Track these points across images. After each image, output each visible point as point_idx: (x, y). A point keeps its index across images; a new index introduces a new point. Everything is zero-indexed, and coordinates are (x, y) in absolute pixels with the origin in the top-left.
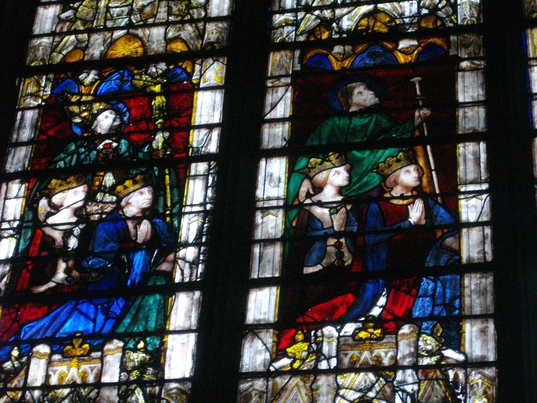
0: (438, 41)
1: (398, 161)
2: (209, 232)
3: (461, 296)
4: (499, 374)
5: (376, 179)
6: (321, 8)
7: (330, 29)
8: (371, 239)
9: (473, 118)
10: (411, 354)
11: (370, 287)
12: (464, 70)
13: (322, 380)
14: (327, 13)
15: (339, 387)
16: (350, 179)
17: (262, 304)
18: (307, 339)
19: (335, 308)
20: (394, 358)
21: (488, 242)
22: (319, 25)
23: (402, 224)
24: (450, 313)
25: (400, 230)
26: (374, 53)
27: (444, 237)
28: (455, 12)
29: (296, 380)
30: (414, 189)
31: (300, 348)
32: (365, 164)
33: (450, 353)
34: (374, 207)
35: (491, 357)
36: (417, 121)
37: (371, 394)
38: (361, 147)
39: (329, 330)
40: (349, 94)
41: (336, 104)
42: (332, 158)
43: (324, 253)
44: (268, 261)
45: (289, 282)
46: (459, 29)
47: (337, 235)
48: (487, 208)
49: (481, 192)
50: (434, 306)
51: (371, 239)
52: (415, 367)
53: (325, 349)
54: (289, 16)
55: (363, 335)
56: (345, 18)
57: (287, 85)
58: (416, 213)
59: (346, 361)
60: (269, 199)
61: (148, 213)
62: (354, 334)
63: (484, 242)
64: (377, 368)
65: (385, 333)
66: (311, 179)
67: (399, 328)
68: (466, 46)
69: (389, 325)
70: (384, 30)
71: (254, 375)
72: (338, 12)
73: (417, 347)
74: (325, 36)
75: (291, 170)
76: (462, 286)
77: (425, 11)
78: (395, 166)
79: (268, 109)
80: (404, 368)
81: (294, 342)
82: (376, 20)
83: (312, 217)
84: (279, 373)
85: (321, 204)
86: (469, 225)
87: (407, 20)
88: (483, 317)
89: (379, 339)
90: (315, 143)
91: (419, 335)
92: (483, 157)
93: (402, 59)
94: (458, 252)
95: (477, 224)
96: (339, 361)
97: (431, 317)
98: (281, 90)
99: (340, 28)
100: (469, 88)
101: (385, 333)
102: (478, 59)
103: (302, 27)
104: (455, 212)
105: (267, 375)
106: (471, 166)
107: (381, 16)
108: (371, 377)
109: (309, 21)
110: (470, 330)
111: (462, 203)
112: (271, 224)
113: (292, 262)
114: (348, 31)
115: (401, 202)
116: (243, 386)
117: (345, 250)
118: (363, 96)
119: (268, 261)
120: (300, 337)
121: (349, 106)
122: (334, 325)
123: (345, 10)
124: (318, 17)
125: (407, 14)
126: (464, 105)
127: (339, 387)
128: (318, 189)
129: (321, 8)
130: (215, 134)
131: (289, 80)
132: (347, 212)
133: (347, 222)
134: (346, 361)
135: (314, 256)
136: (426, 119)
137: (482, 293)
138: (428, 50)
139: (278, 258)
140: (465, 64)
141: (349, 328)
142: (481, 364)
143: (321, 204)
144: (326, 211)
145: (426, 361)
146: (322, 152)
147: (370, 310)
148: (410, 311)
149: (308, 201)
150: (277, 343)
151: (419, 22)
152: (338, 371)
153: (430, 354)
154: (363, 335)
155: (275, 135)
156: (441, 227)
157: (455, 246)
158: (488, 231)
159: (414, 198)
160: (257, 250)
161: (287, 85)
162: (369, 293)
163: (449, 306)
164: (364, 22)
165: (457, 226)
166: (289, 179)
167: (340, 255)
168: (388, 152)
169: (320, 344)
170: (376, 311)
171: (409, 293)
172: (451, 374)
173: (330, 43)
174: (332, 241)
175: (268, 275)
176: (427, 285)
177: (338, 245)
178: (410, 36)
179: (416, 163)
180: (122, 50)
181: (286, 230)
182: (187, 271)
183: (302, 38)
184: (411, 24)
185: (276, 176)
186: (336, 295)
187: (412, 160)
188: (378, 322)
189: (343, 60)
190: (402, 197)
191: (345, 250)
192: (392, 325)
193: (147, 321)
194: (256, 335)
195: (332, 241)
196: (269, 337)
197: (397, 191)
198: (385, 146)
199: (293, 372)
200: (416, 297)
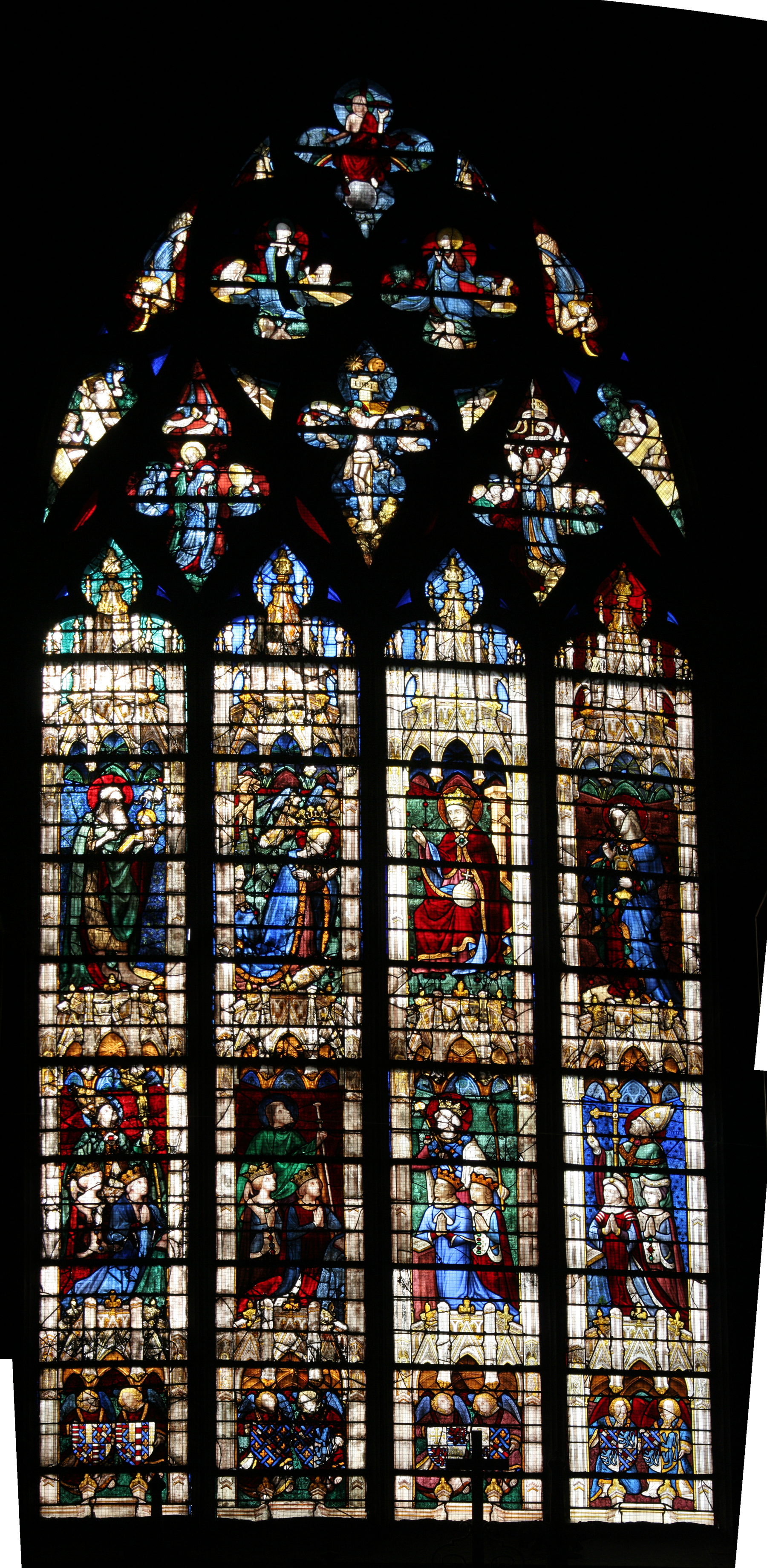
0: (332, 1072)
1: (307, 1174)
2: (189, 1219)
3: (345, 1284)
4: (367, 1341)
5: (293, 1187)
6: (251, 1026)
7: (257, 1048)
8: (291, 1235)
9: (354, 1145)
10: (316, 1323)
11: (291, 1271)
12: (348, 1100)
13: (265, 1336)
14: (254, 1032)
15: (275, 1342)
16: (276, 1185)
17: (226, 1279)
18: (254, 1307)
19: (271, 1286)
20: (306, 1324)
21: (361, 1245)
22: (249, 1043)
23: (308, 1226)
24: (338, 1295)
25: (309, 1230)
26: (289, 1076)
27: (335, 1239)
28: (343, 1045)
29: (249, 1335)
30: (316, 1198)
31: (250, 1313)
32: (286, 1174)
33: (338, 1323)
34: (292, 1210)
35: (362, 1330)
36: (318, 1142)
37: (294, 1348)
38: (283, 1160)
39: (268, 1301)
40: (273, 1112)
41: (264, 1119)
42: (264, 1166)
43: (262, 1244)
44: (227, 1247)
45: (241, 1263)
46: (347, 1063)
47: (269, 1230)
48: (361, 1219)
49: (358, 1206)
50: (330, 1289)
51: (291, 1235)
52: (319, 1332)
53: (266, 1315)
54: (227, 1030)
55: (288, 1306)
56: (267, 1038)
57: (230, 1097)
58: (318, 1218)
59: (279, 1323)
60: (225, 1196)
61: (147, 1199)
62: (283, 1305)
63: (359, 1245)
64: (297, 1331)
65: (301, 1306)
66: (251, 1182)
67: (309, 1304)
68: (350, 1079)
69: (303, 1301)
70: (295, 1055)
71: (224, 1330)
72: (264, 1031)
73: (319, 1318)
74: (254, 1055)
75: (238, 1174)
76: (346, 1277)
77: (322, 1040)
78: (305, 1178)
79: (219, 1118)
80: (312, 1332)
81: (247, 1308)
82: (289, 1044)
83: (253, 1214)
84: (239, 1329)
85: (259, 1205)
86: (351, 1231)
87: (310, 1047)
88: (358, 1301)
89: (297, 1310)
90: (253, 1152)
91: (321, 1309)
92: (360, 1177)
93: (307, 1084)
94: (344, 1251)
95: (355, 1231)
96: (275, 1324)
97: (328, 1298)
98: (226, 1101)
99: (264, 1047)
100: (352, 1118)
101: (301, 1306)
102: (358, 1092)
103: (237, 1044)
104: (342, 1221)
105: (233, 1330)
106: (352, 1184)
107: (292, 1040)
108: (293, 1336)
109: (242, 1038)
110: (350, 1308)
111: (346, 1212)
112: (227, 1217)
113: (242, 1248)
114: (270, 1052)
115: (308, 1208)
116: (219, 1337)
117: (275, 1242)
118: (283, 1115)
119: (227, 1247)
120: (251, 1305)
121: (273, 1123)
122: (270, 1298)
123: (267, 1030)
124: (248, 1035)
125: (310, 1042)
126: (349, 1132)
127: (275, 1342)
128: (256, 1191)
129: (251, 1026)
130: (185, 1134)
131: (230, 1093)
132: (275, 1212)
133: (276, 1221)
134: (279, 1323)
135: (256, 1245)
136: (324, 1141)
137: (358, 1283)
138: (325, 1078)
139: (233, 1244)
140: (349, 1095)
141: (280, 1301)
142: (356, 1333)
143: (259, 1205)
144: (262, 1210)
145: (325, 1328)
146: (257, 1160)
147: (291, 1289)
148: (315, 1292)
149: (250, 1201)
150: (237, 1308)
151: (318, 1051)
152: (274, 1331)
153: (328, 1323)
154: (288, 1306)
155: (225, 1142)
156: (334, 1231)
157: (342, 1246)
158: (361, 1236)
159: (317, 1206)
160: (220, 1236)
161: (230, 1097)
162: (290, 1278)
163: (338, 1291)
164: (281, 1044)
165: (343, 1231)
166: (237, 1180)
167: (272, 1245)
168: (300, 1166)
169: (262, 1310)
170: (295, 1290)
171: (314, 1279)
172: (339, 1338)
173: (257, 1063)
174: (267, 1235)
175: (228, 1258)
176: (325, 1274)
177: (270, 1238)
178: (312, 1064)
179: (318, 1178)
180: (112, 1048)
181: (237, 1222)
182: (176, 1249)
183: (238, 1054)
184: (313, 1051)
185: (228, 1177)
186: (270, 1277)
187: (316, 1176)
188: (297, 1298)
189: (267, 1079)
190: (310, 1205)
191: (275, 1242)
192: (305, 1301)
193: (155, 1283)
194: (223, 1301)
195: (267, 1235)
196: (231, 1303)
197: (307, 1200)
198: (298, 1160)
199: (248, 1329)
200: (319, 1282)
